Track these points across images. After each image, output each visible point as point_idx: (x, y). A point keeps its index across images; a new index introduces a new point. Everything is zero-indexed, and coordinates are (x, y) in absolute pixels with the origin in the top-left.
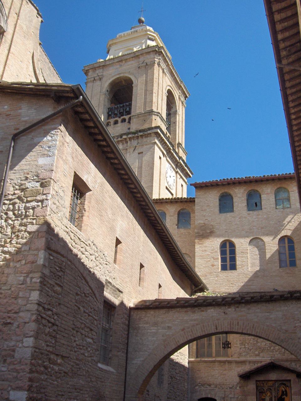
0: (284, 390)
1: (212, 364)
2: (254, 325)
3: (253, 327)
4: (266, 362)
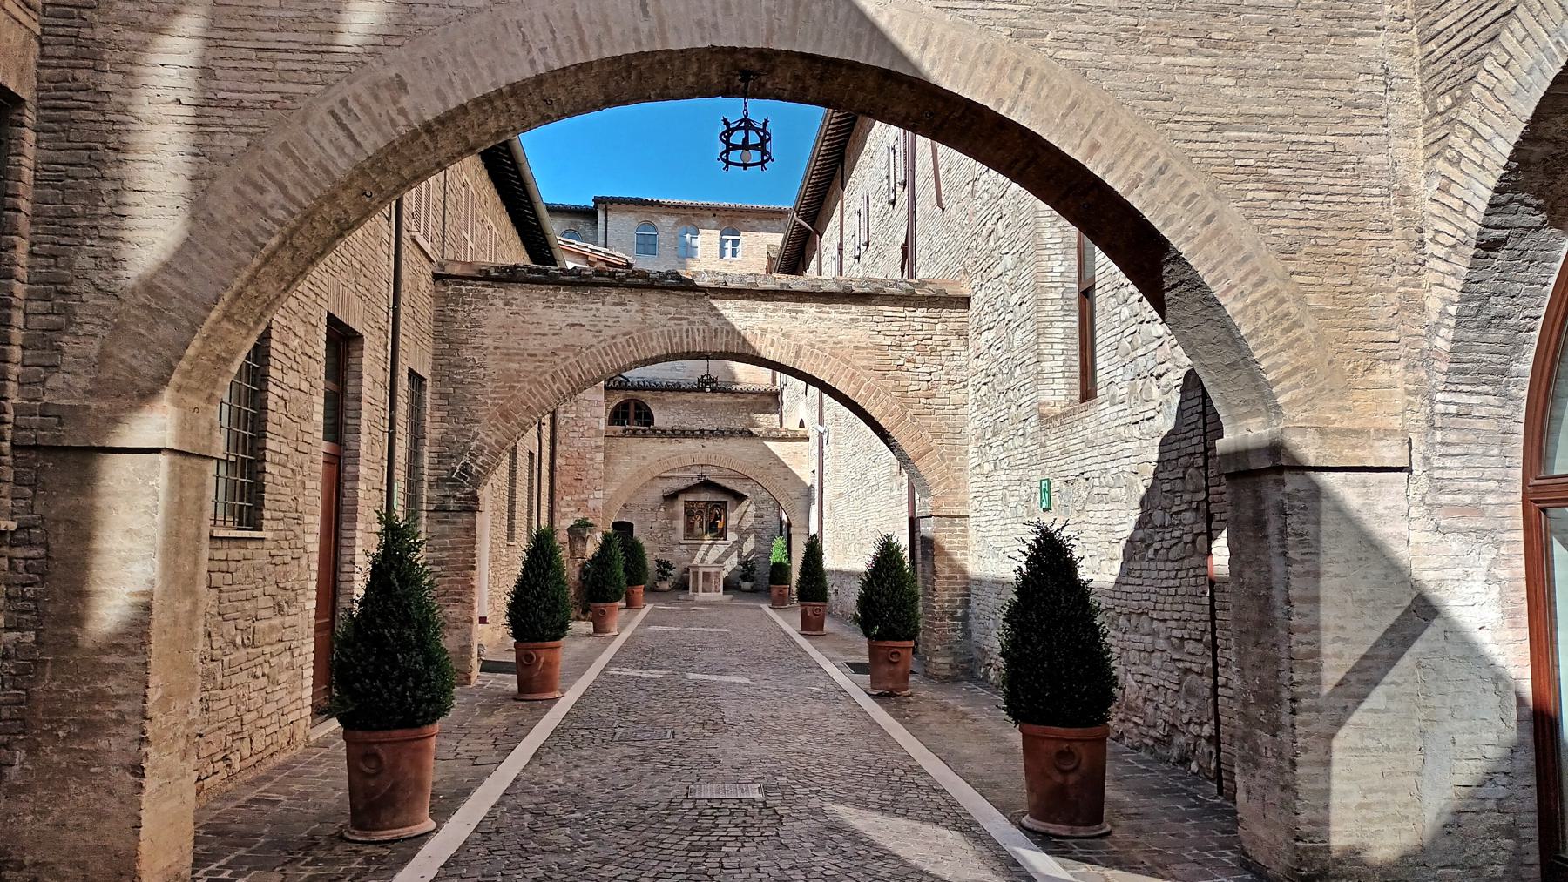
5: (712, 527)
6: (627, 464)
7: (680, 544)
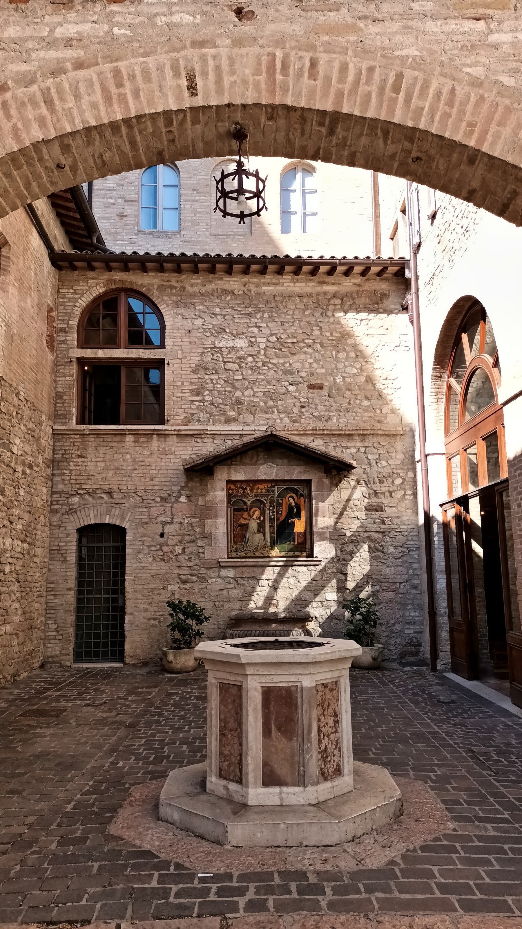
0: (293, 504)
1: (118, 439)
2: (400, 76)
3: (396, 89)
4: (255, 436)
7: (220, 566)
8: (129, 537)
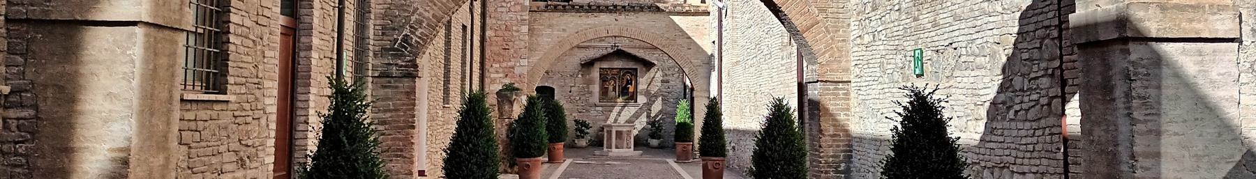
5: (624, 91)
6: (549, 36)
7: (596, 106)
8: (555, 92)
